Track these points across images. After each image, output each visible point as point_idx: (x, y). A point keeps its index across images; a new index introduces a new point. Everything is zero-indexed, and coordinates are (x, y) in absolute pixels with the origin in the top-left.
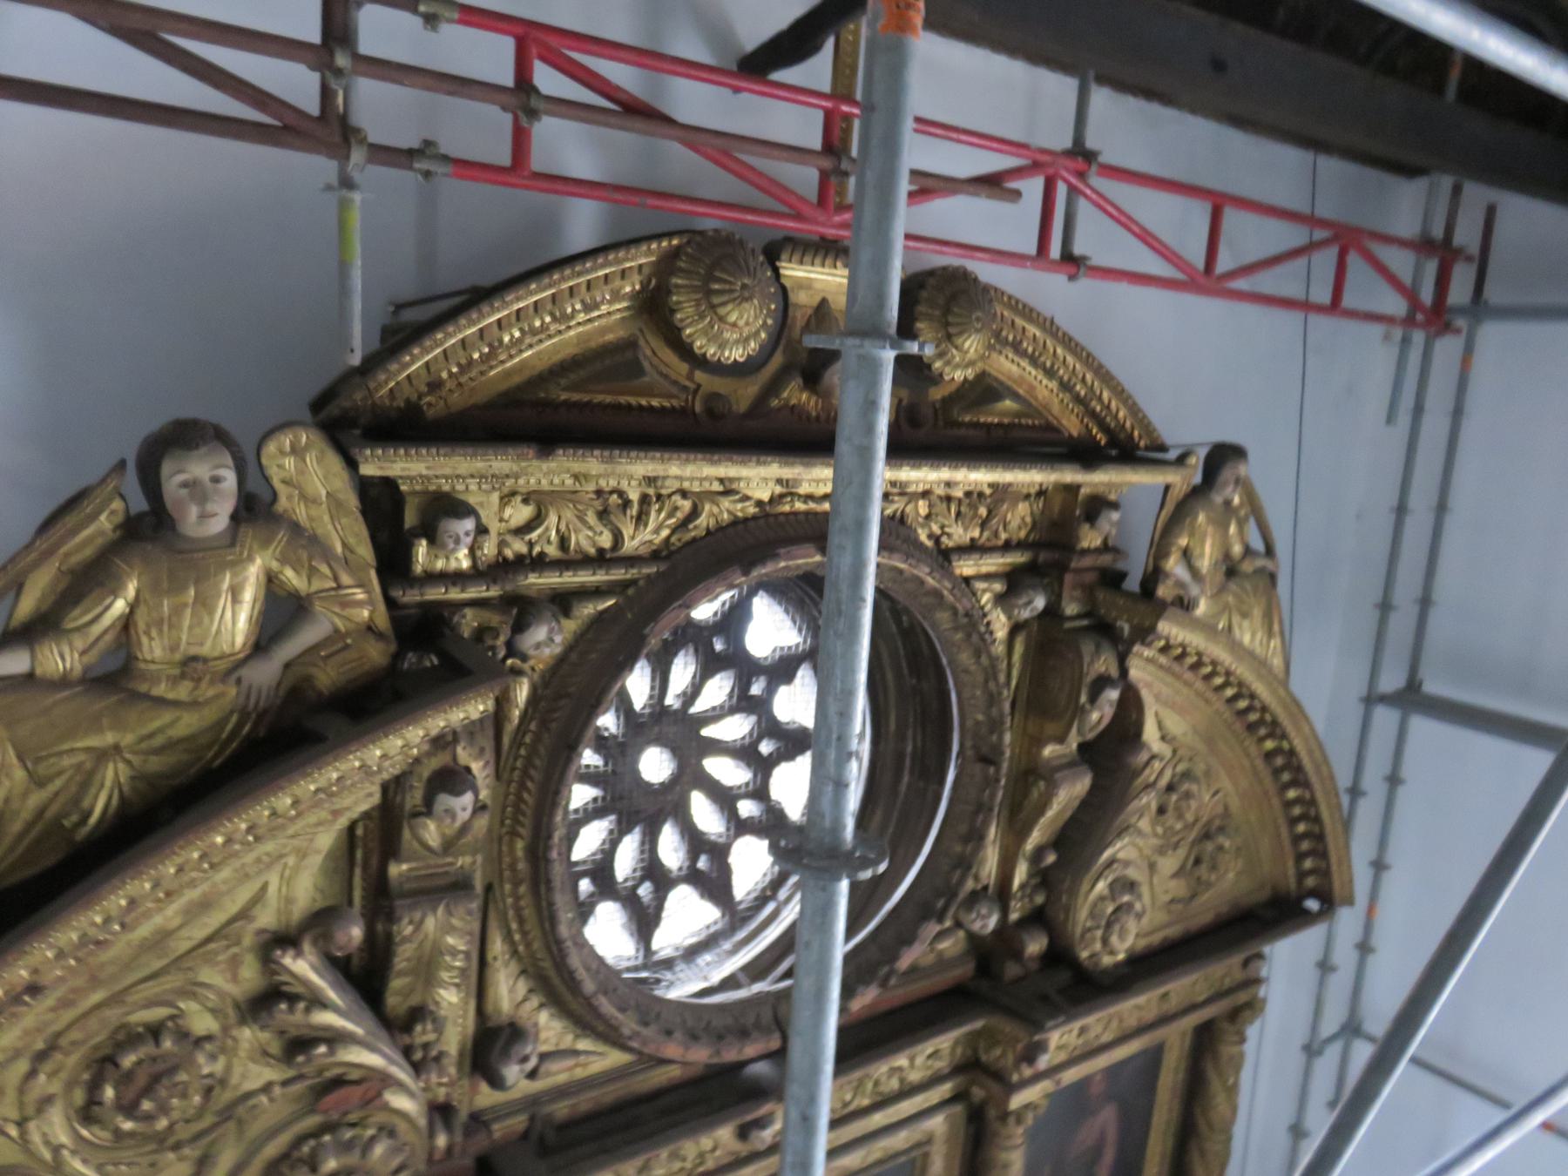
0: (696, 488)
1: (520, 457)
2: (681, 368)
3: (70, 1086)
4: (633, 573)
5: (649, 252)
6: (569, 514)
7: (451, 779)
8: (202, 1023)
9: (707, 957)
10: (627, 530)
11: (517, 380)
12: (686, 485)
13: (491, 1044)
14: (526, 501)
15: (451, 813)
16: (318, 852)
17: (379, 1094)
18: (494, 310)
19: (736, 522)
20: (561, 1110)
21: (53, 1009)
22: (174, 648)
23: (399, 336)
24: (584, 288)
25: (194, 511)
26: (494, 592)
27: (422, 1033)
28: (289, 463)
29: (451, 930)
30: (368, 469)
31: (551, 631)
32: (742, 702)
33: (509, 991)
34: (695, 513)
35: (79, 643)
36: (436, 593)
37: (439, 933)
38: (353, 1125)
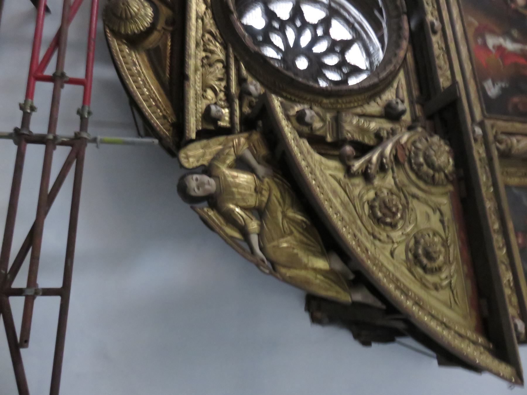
0: (200, 32)
1: (189, 86)
2: (155, 36)
3: (384, 230)
4: (232, 56)
5: (113, 41)
6: (210, 77)
7: (300, 117)
8: (371, 195)
9: (371, 49)
10: (216, 57)
11: (162, 92)
12: (200, 35)
13: (391, 114)
14: (205, 91)
15: (312, 117)
16: (321, 159)
17: (402, 145)
18: (137, 95)
19: (214, 18)
20: (416, 93)
21: (361, 234)
22: (252, 195)
23: (148, 129)
24: (128, 66)
25: (207, 187)
26: (237, 101)
27: (384, 134)
28: (191, 160)
29: (351, 122)
30: (193, 136)
31: (251, 83)
32: (282, 31)
33: (374, 108)
34: (210, 33)
35: (248, 220)
36: (237, 120)
37: (351, 125)
38: (410, 153)
